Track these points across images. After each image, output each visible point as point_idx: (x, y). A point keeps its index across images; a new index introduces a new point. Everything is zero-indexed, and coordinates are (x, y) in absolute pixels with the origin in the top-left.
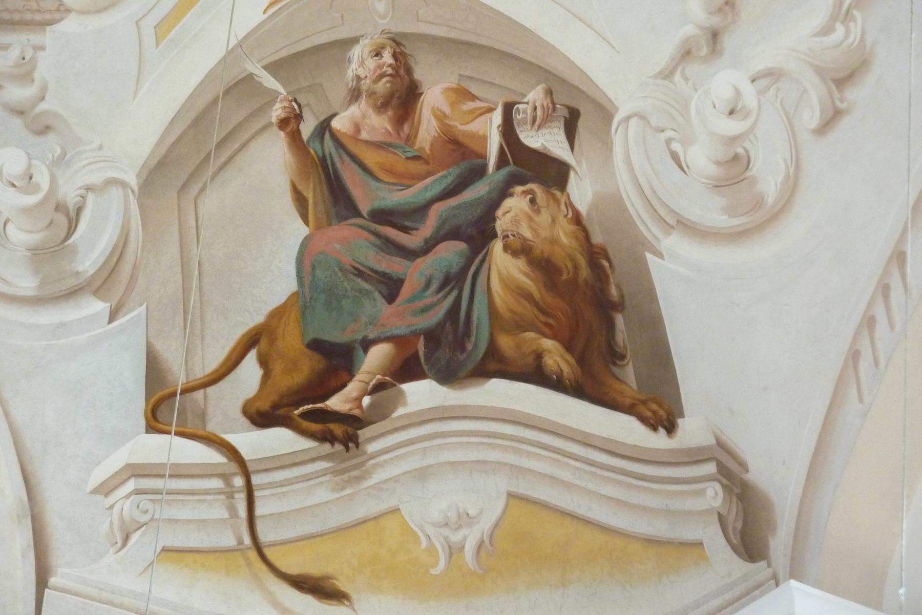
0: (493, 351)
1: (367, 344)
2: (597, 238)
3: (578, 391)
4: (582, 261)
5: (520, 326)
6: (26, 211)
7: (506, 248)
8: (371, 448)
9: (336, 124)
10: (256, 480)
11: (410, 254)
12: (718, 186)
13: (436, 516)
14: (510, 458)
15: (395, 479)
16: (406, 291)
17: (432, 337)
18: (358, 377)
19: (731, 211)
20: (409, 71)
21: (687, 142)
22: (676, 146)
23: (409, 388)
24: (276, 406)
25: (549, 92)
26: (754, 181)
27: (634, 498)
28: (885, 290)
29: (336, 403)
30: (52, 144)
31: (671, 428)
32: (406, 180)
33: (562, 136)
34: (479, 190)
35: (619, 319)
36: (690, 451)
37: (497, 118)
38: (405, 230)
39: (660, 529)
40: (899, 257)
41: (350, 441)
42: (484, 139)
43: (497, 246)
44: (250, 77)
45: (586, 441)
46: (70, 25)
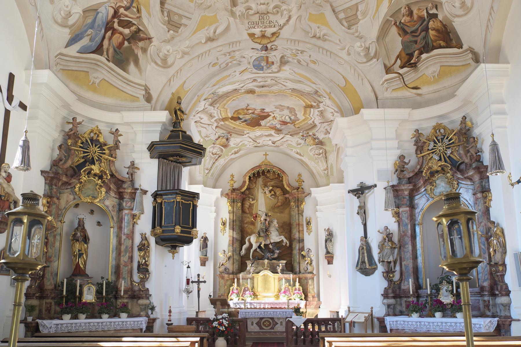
0: (433, 46)
1: (414, 52)
2: (444, 23)
3: (447, 47)
4: (443, 28)
5: (436, 41)
6: (362, 50)
7: (431, 30)
8: (419, 66)
9: (402, 21)
10: (403, 76)
11: (417, 36)
12: (461, 8)
13: (430, 73)
14: (439, 61)
15: (423, 69)
16: (418, 42)
17: (424, 47)
18: (415, 57)
19: (464, 11)
20: (410, 9)
21: (455, 3)
22: (453, 4)
23: (421, 56)
24: (404, 65)
25: (432, 4)
26: (466, 5)
27: (459, 60)
28: (491, 14)
29: (412, 62)
30: (363, 40)
31: (462, 48)
32: (414, 25)
33: (435, 10)
34: (425, 23)
35: (450, 34)
36: (465, 50)
37: (425, 11)
38: (416, 33)
39: (464, 63)
40: (492, 8)
41: (416, 66)
42: (424, 15)
43: (430, 30)
44: (388, 19)
45: (450, 54)
46: (361, 22)
